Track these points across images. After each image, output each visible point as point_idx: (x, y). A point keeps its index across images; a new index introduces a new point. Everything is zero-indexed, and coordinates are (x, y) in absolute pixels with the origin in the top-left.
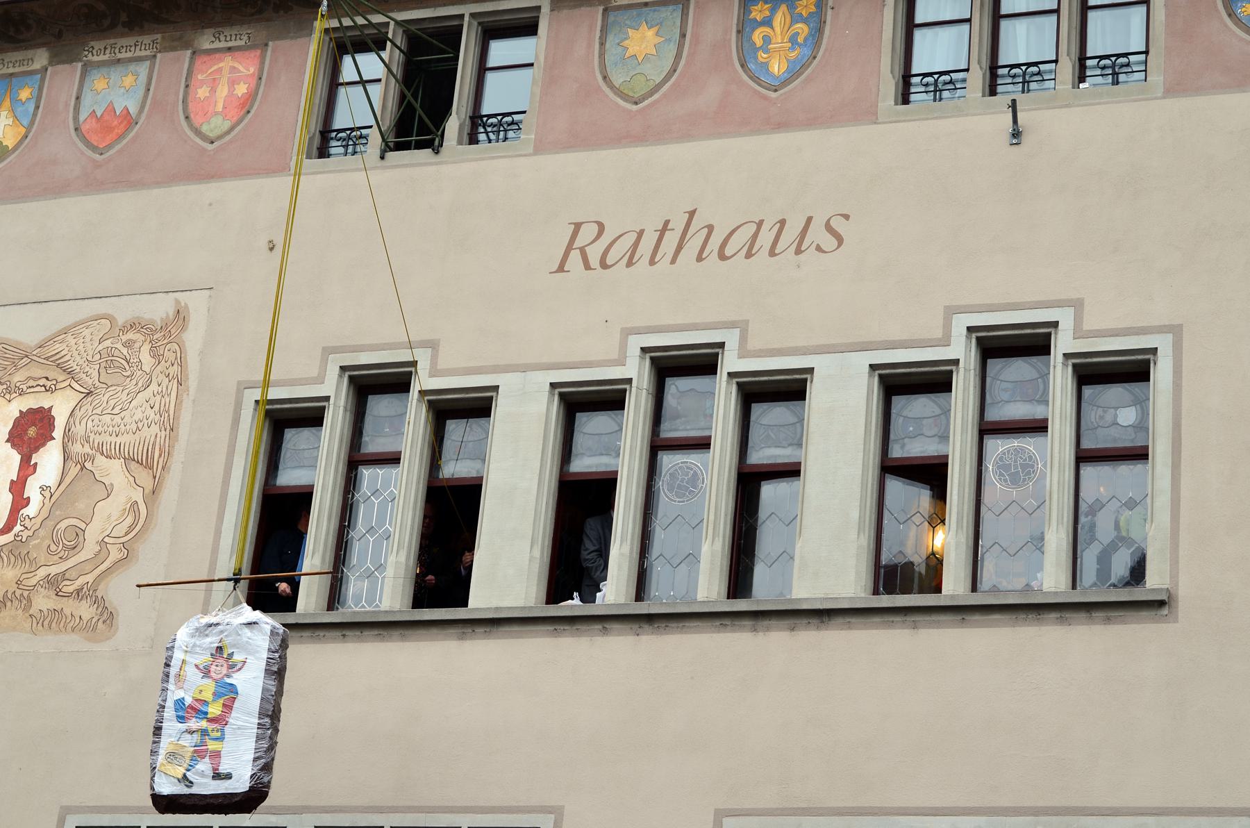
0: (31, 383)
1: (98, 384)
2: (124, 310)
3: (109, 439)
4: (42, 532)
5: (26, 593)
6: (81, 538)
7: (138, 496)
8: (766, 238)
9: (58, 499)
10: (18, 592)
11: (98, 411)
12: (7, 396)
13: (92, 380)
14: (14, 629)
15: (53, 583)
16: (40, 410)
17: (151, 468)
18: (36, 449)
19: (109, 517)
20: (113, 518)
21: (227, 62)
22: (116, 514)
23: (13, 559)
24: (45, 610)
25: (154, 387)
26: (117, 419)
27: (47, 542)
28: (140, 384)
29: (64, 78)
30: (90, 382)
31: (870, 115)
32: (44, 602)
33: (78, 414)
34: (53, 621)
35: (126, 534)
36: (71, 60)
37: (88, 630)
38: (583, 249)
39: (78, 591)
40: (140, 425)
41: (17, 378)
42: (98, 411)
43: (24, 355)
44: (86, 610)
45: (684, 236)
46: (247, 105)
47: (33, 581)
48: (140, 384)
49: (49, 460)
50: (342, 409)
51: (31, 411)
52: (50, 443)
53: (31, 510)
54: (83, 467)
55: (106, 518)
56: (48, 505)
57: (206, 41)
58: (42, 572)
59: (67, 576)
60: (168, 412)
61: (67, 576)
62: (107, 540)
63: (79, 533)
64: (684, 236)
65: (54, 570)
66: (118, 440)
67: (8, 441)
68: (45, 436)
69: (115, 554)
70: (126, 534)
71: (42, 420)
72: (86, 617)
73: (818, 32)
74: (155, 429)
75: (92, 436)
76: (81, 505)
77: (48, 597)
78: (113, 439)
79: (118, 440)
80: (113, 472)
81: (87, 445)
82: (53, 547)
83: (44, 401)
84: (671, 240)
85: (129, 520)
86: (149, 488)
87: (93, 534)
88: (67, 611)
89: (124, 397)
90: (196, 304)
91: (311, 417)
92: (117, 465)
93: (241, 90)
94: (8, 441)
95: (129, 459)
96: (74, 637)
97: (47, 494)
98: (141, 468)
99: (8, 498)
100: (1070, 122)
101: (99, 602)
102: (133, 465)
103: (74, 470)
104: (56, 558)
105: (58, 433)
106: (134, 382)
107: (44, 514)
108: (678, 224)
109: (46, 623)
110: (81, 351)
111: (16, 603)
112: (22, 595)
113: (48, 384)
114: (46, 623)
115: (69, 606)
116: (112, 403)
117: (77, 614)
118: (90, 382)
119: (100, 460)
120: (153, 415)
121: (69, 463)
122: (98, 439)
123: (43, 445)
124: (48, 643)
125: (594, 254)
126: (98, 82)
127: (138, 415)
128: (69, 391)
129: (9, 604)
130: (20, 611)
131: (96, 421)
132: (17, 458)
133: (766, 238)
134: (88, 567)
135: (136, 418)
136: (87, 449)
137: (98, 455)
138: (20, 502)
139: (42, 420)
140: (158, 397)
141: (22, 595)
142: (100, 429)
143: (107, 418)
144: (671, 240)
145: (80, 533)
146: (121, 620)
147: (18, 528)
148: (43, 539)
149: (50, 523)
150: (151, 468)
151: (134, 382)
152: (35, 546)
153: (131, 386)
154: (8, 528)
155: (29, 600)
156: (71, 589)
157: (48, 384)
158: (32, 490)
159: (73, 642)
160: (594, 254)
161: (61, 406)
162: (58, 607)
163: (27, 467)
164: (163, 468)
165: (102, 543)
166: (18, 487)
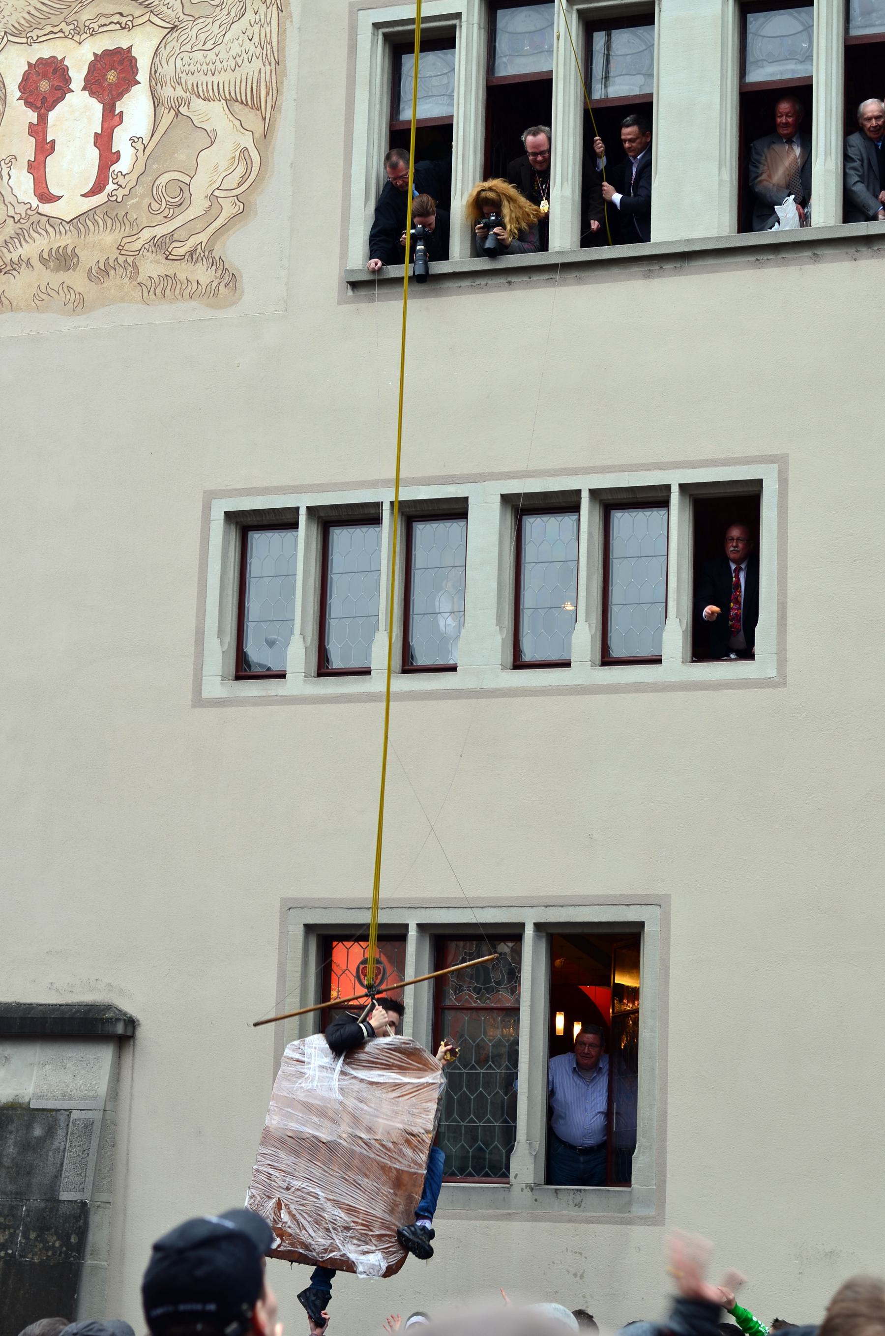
0: (103, 21)
1: (182, 17)
3: (204, 79)
4: (139, 190)
5: (130, 260)
6: (187, 194)
7: (247, 141)
9: (153, 151)
10: (121, 259)
11: (187, 47)
12: (77, 38)
13: (175, 12)
14: (122, 300)
16: (118, 51)
17: (259, 109)
18: (120, 96)
19: (216, 167)
20: (221, 169)
22: (224, 164)
23: (109, 222)
24: (155, 276)
25: (249, 16)
26: (211, 55)
27: (147, 201)
28: (233, 14)
30: (173, 15)
32: (152, 267)
33: (164, 53)
34: (166, 288)
35: (240, 185)
37: (208, 295)
39: (191, 253)
40: (239, 61)
41: (85, 16)
42: (187, 47)
44: (203, 274)
47: (137, 245)
48: (233, 14)
49: (136, 108)
50: (476, 26)
51: (106, 53)
52: (135, 89)
53: (123, 166)
54: (178, 113)
55: (213, 169)
56: (142, 159)
58: (146, 235)
59: (176, 237)
60: (270, 43)
61: (176, 237)
62: (217, 193)
63: (184, 188)
65: (160, 231)
66: (216, 79)
67: (84, 89)
68: (128, 80)
69: (229, 209)
70: (240, 185)
71: (121, 62)
72: (204, 281)
74: (257, 64)
75: (184, 77)
76: (181, 156)
77: (157, 262)
78: (209, 78)
79: (216, 79)
80: (213, 115)
81: (179, 88)
82: (155, 206)
83: (122, 41)
85: (241, 169)
86: (259, 132)
87: (200, 187)
88: (182, 276)
89: (216, 31)
91: (441, 38)
92: (218, 107)
94: (84, 89)
95: (230, 101)
96: (193, 304)
97: (140, 146)
98: (246, 109)
99: (94, 154)
101: (215, 262)
102: (237, 107)
103: (168, 118)
104: (160, 217)
105: (143, 76)
106: (225, 12)
107: (139, 168)
109: (158, 290)
111: (120, 271)
112: (126, 261)
113: (123, 20)
114: (158, 290)
115: (183, 271)
116: (202, 37)
117: (193, 278)
118: (173, 15)
119: (197, 103)
120: (252, 49)
121: (161, 110)
122: (191, 80)
123: (127, 90)
124: (164, 314)
127: (236, 50)
128: (149, 27)
129: (112, 272)
130: (126, 280)
131: (186, 59)
132: (97, 108)
134: (199, 226)
135: (233, 52)
136: (179, 92)
137: (194, 98)
139: (121, 62)
140: (257, 28)
141: (126, 261)
142: (192, 68)
143: (199, 55)
145: (185, 188)
146: (246, 282)
147: (110, 187)
148: (142, 197)
149: (148, 179)
150: (259, 109)
151: (225, 12)
152: (131, 206)
153: (222, 16)
155: (135, 266)
156: (182, 251)
157: (123, 20)
158: (121, 141)
161: (142, 45)
162: (170, 273)
163: (112, 117)
164: (273, 108)
165: (212, 197)
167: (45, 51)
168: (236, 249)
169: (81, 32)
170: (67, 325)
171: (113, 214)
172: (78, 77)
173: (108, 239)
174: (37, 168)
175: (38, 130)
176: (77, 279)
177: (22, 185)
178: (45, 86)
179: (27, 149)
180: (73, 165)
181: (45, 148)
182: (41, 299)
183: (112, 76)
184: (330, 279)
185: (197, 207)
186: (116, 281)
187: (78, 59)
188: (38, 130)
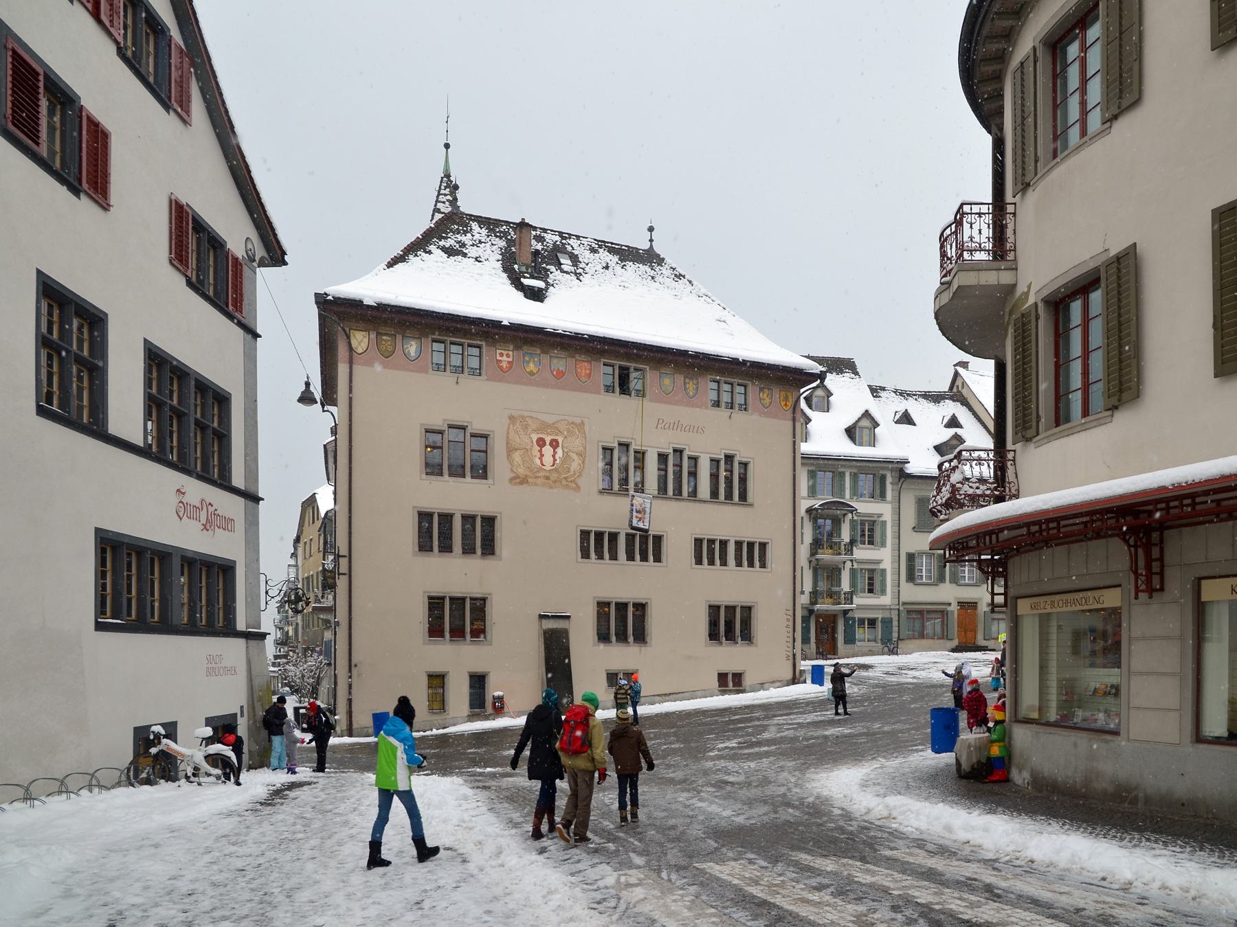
2: (571, 419)
15: (566, 478)
29: (545, 359)
31: (707, 408)
32: (564, 482)
34: (567, 487)
36: (546, 352)
43: (549, 426)
46: (589, 375)
49: (559, 450)
55: (575, 466)
57: (577, 356)
64: (676, 426)
80: (574, 456)
87: (572, 469)
90: (586, 421)
100: (738, 416)
110: (562, 426)
126: (555, 361)
138: (555, 460)
161: (560, 440)
166: (554, 456)
168: (580, 482)
174: (541, 459)
175: (540, 451)
177: (538, 462)
178: (541, 443)
180: (548, 459)
181: (542, 455)
184: (595, 489)
187: (548, 439)
188: (540, 451)
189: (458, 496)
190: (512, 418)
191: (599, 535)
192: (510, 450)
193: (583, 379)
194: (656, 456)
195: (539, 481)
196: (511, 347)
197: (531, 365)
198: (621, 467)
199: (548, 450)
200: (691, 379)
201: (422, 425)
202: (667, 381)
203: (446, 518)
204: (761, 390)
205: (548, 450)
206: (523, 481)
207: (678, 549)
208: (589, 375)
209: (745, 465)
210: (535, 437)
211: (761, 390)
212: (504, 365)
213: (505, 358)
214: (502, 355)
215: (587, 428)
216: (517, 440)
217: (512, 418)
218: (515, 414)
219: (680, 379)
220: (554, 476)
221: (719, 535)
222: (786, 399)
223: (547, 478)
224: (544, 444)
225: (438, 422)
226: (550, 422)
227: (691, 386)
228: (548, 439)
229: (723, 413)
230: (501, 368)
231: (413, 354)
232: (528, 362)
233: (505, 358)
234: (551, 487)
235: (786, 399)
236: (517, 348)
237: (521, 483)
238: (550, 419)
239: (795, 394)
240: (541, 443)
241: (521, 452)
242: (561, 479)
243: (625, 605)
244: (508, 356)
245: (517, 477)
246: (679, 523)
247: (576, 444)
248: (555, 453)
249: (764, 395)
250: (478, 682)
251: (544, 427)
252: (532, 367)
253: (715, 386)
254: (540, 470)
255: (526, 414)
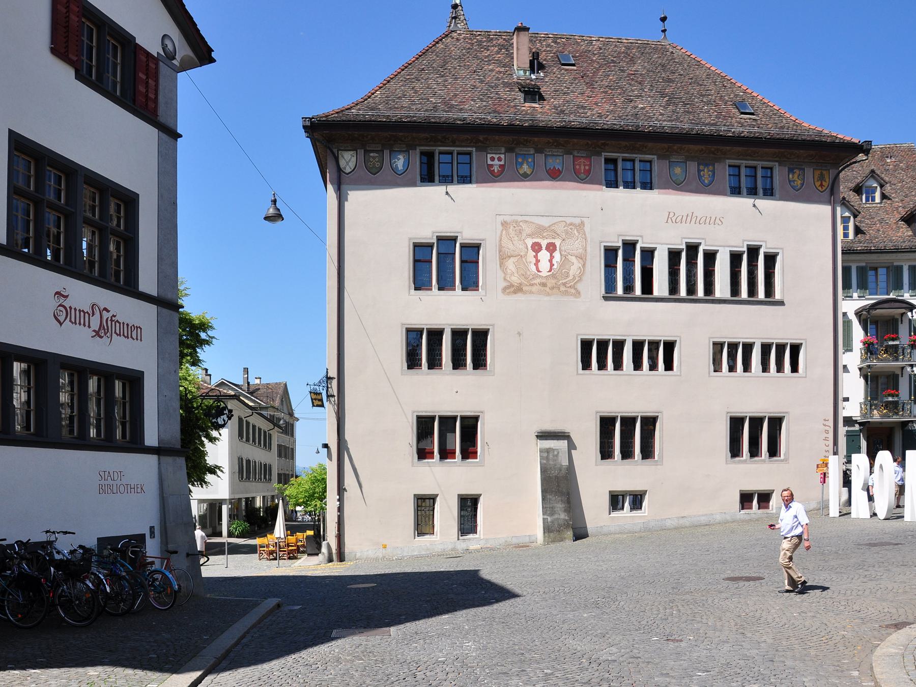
2: (569, 220)
8: (708, 221)
9: (562, 265)
15: (564, 284)
21: (582, 160)
29: (540, 158)
32: (563, 289)
34: (566, 293)
36: (541, 152)
38: (672, 218)
44: (573, 291)
45: (690, 218)
49: (557, 255)
53: (555, 267)
73: (714, 174)
80: (573, 259)
84: (689, 218)
87: (571, 273)
93: (587, 168)
108: (690, 215)
110: (560, 229)
115: (569, 290)
125: (674, 219)
133: (708, 221)
138: (552, 265)
144: (689, 218)
154: (550, 271)
158: (554, 261)
159: (572, 299)
160: (674, 219)
161: (558, 243)
166: (551, 261)
167: (537, 240)
168: (580, 286)
169: (543, 237)
170: (546, 298)
171: (554, 276)
172: (544, 247)
173: (554, 281)
174: (536, 264)
175: (536, 257)
176: (547, 289)
177: (534, 268)
178: (537, 248)
179: (534, 260)
180: (544, 265)
181: (538, 261)
182: (539, 293)
183: (551, 248)
185: (571, 277)
186: (555, 290)
187: (544, 243)
188: (536, 257)
189: (448, 309)
190: (504, 224)
191: (603, 345)
192: (503, 258)
193: (583, 176)
194: (666, 253)
195: (534, 289)
196: (503, 150)
197: (525, 166)
198: (627, 268)
199: (544, 255)
200: (706, 165)
201: (410, 239)
202: (678, 170)
203: (435, 335)
204: (791, 170)
205: (544, 255)
206: (518, 289)
207: (693, 355)
208: (588, 172)
209: (771, 260)
210: (530, 242)
211: (791, 170)
212: (496, 169)
213: (496, 162)
214: (493, 159)
215: (587, 228)
216: (511, 246)
217: (504, 224)
218: (508, 219)
219: (693, 166)
220: (551, 282)
221: (741, 336)
222: (822, 178)
223: (544, 285)
224: (540, 249)
225: (427, 235)
226: (547, 225)
227: (706, 173)
228: (544, 243)
229: (744, 202)
230: (492, 172)
231: (400, 167)
232: (522, 164)
233: (496, 162)
234: (548, 295)
235: (822, 178)
236: (510, 150)
237: (515, 292)
238: (545, 222)
239: (833, 172)
240: (537, 248)
241: (512, 260)
242: (561, 285)
243: (633, 420)
244: (499, 159)
245: (511, 286)
246: (694, 326)
247: (574, 245)
248: (552, 257)
249: (795, 177)
250: (468, 506)
251: (540, 230)
252: (525, 168)
253: (734, 171)
254: (535, 277)
255: (520, 218)
